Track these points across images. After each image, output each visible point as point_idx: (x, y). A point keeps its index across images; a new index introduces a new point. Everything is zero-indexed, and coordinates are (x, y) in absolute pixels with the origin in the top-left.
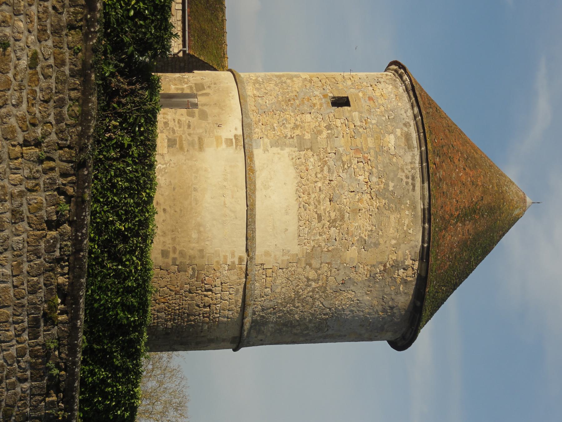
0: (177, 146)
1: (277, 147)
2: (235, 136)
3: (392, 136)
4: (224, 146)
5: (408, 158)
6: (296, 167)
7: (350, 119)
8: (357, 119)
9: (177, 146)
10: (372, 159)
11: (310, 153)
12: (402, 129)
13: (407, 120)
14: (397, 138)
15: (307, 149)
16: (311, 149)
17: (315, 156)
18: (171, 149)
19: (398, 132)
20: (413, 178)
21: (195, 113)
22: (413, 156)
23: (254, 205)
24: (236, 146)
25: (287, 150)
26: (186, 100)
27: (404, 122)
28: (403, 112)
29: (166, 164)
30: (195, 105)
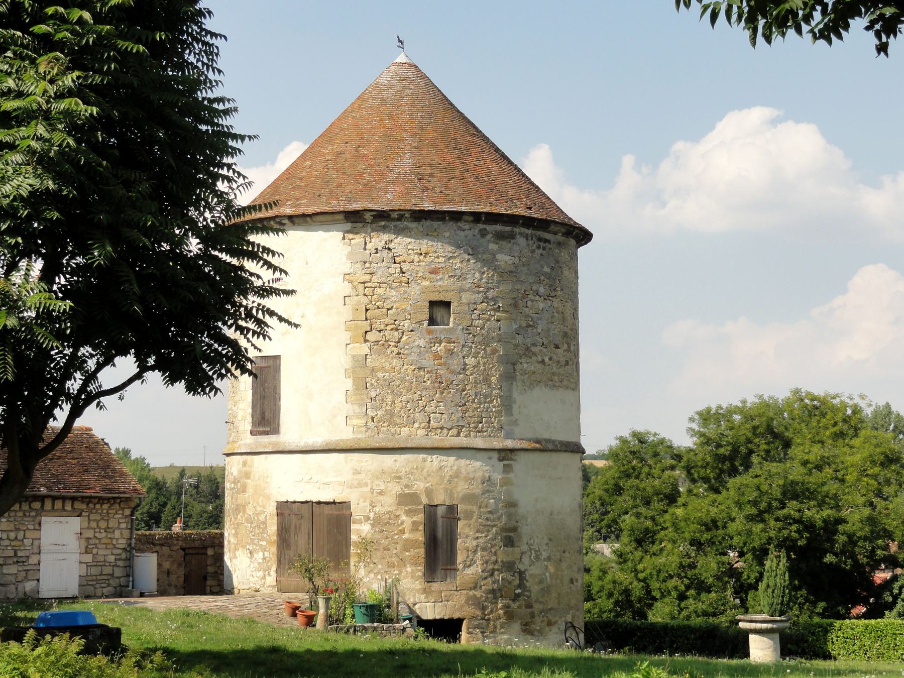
0: (512, 534)
1: (512, 408)
2: (500, 460)
3: (499, 256)
4: (511, 475)
5: (521, 241)
6: (532, 386)
7: (473, 306)
8: (473, 297)
9: (512, 534)
10: (524, 289)
11: (518, 367)
12: (489, 241)
13: (477, 231)
14: (501, 250)
15: (515, 370)
16: (514, 364)
17: (523, 360)
18: (516, 544)
19: (493, 247)
20: (540, 239)
21: (466, 511)
22: (520, 234)
23: (562, 443)
24: (512, 460)
25: (515, 395)
26: (440, 522)
27: (479, 236)
28: (462, 233)
29: (531, 549)
30: (452, 509)
